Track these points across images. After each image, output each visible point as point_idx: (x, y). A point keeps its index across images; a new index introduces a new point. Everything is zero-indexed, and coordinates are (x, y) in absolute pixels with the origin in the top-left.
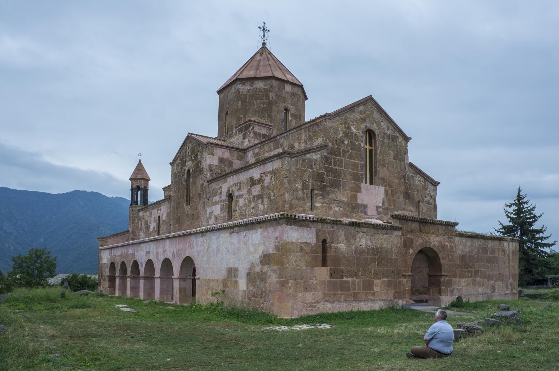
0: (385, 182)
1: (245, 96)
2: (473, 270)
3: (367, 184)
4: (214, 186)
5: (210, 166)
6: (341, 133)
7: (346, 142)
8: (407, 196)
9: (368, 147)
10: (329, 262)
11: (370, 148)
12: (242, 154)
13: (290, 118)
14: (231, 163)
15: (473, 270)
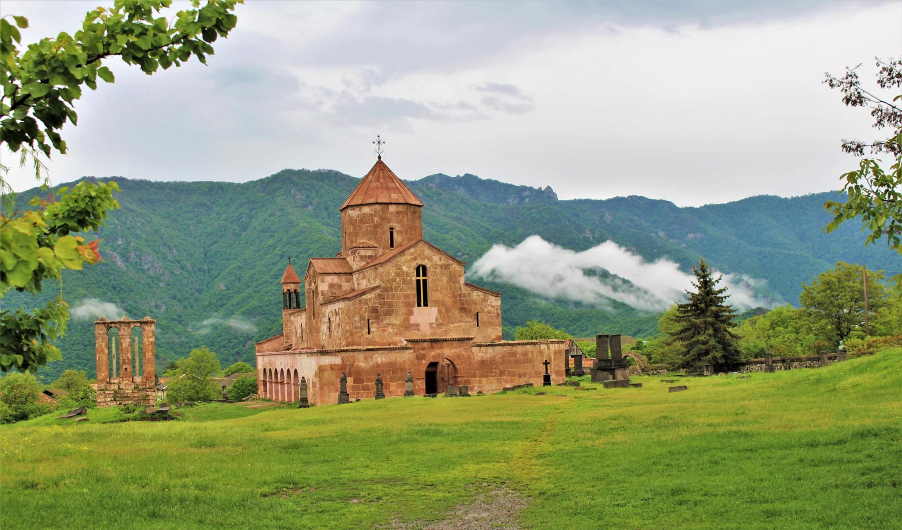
0: (437, 303)
1: (356, 220)
2: (498, 371)
3: (421, 306)
4: (324, 309)
5: (322, 291)
6: (393, 274)
7: (398, 280)
8: (463, 310)
9: (421, 278)
10: (353, 375)
11: (424, 278)
12: (349, 277)
13: (395, 235)
14: (340, 286)
15: (498, 371)
